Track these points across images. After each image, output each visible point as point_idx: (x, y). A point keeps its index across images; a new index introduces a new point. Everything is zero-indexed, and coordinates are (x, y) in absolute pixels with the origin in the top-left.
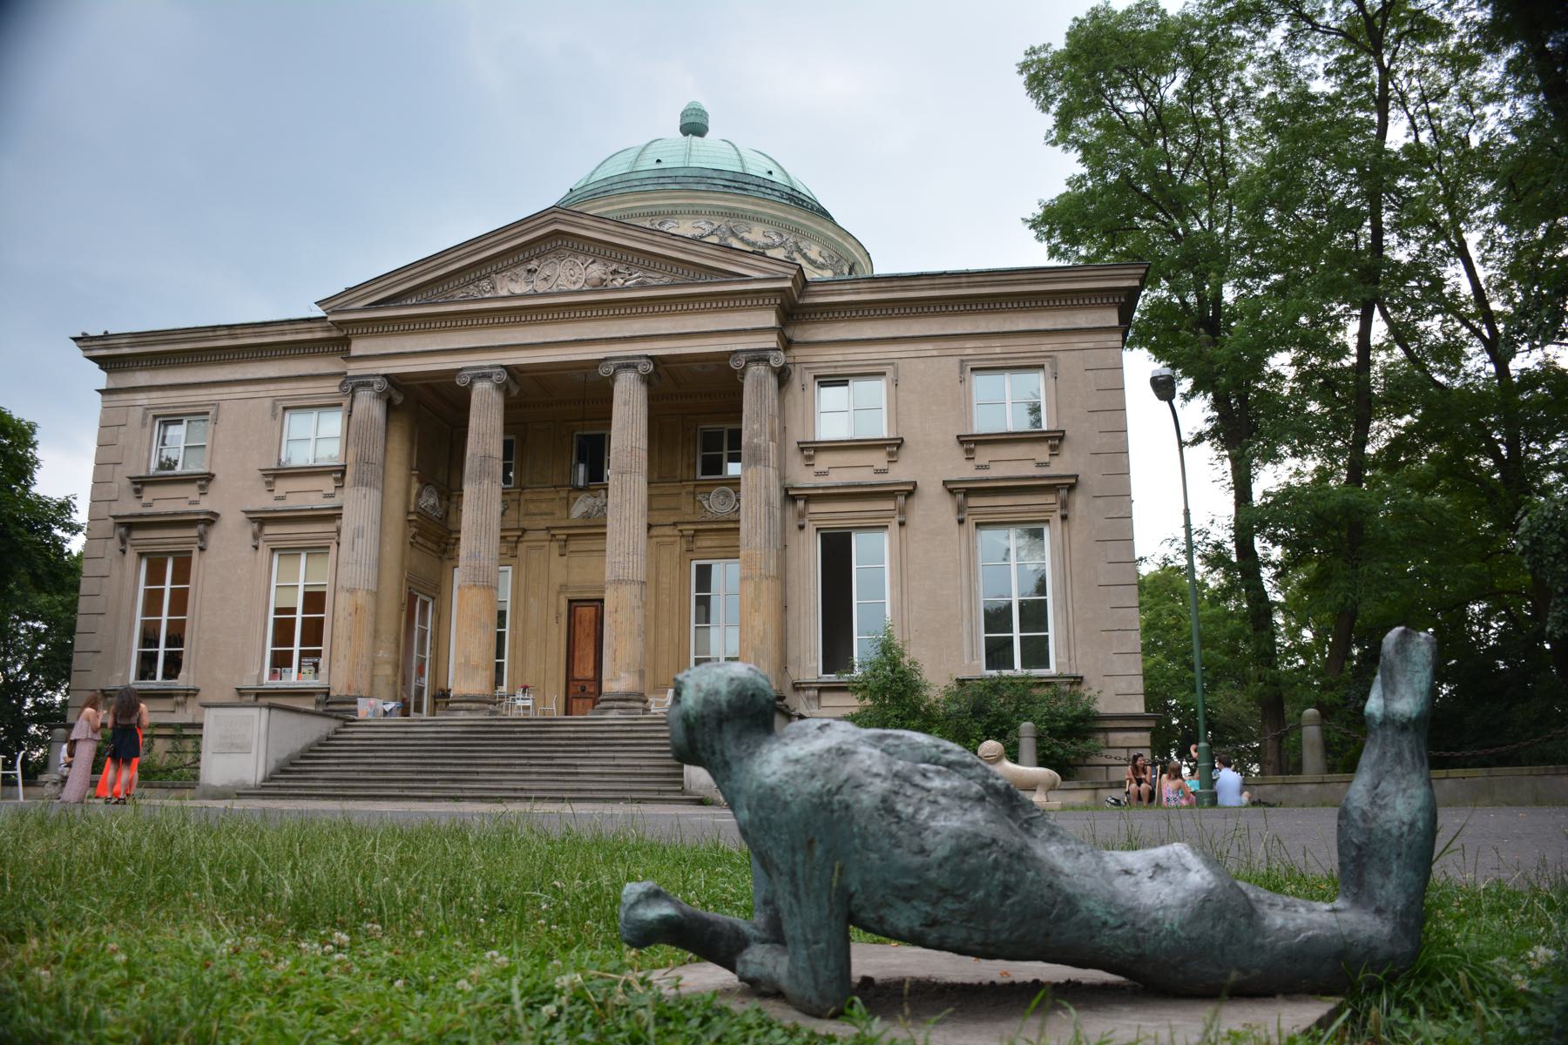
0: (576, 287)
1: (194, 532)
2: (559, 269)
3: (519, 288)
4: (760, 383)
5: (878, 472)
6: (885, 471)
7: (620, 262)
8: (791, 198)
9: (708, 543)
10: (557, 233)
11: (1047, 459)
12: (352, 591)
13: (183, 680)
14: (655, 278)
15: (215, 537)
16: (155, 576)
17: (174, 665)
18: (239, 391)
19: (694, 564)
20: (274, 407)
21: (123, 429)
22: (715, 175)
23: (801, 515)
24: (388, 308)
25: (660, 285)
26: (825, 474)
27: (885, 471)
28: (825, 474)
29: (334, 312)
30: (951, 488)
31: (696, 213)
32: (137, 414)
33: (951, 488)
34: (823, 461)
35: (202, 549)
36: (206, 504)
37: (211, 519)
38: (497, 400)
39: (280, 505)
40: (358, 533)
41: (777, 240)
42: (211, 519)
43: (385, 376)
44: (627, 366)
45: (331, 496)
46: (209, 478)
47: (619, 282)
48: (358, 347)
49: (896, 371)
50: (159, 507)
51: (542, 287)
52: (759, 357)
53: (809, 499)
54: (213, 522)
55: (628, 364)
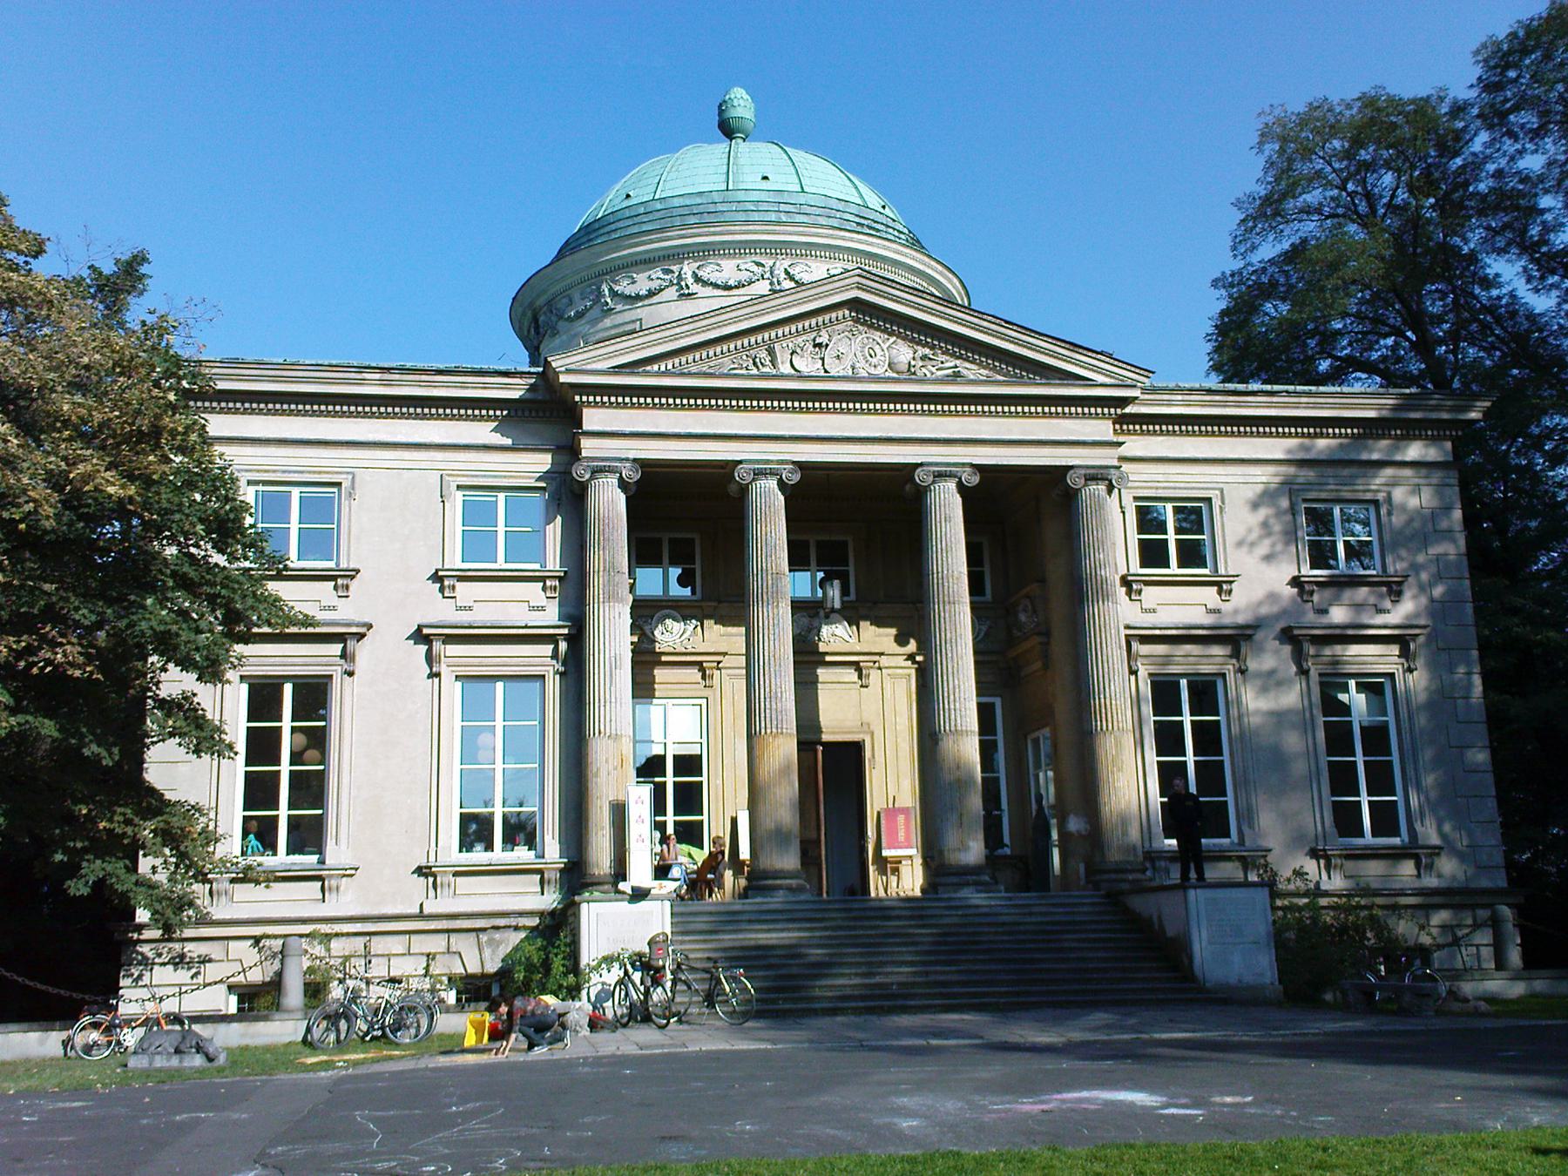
0: (879, 371)
1: (336, 649)
3: (806, 364)
5: (1210, 611)
7: (926, 345)
12: (616, 737)
14: (970, 370)
17: (308, 836)
22: (841, 206)
25: (976, 377)
29: (568, 371)
34: (1151, 595)
35: (351, 674)
39: (464, 617)
40: (616, 665)
43: (635, 460)
44: (951, 475)
45: (543, 609)
46: (353, 574)
47: (929, 371)
48: (593, 418)
52: (1097, 475)
54: (362, 636)
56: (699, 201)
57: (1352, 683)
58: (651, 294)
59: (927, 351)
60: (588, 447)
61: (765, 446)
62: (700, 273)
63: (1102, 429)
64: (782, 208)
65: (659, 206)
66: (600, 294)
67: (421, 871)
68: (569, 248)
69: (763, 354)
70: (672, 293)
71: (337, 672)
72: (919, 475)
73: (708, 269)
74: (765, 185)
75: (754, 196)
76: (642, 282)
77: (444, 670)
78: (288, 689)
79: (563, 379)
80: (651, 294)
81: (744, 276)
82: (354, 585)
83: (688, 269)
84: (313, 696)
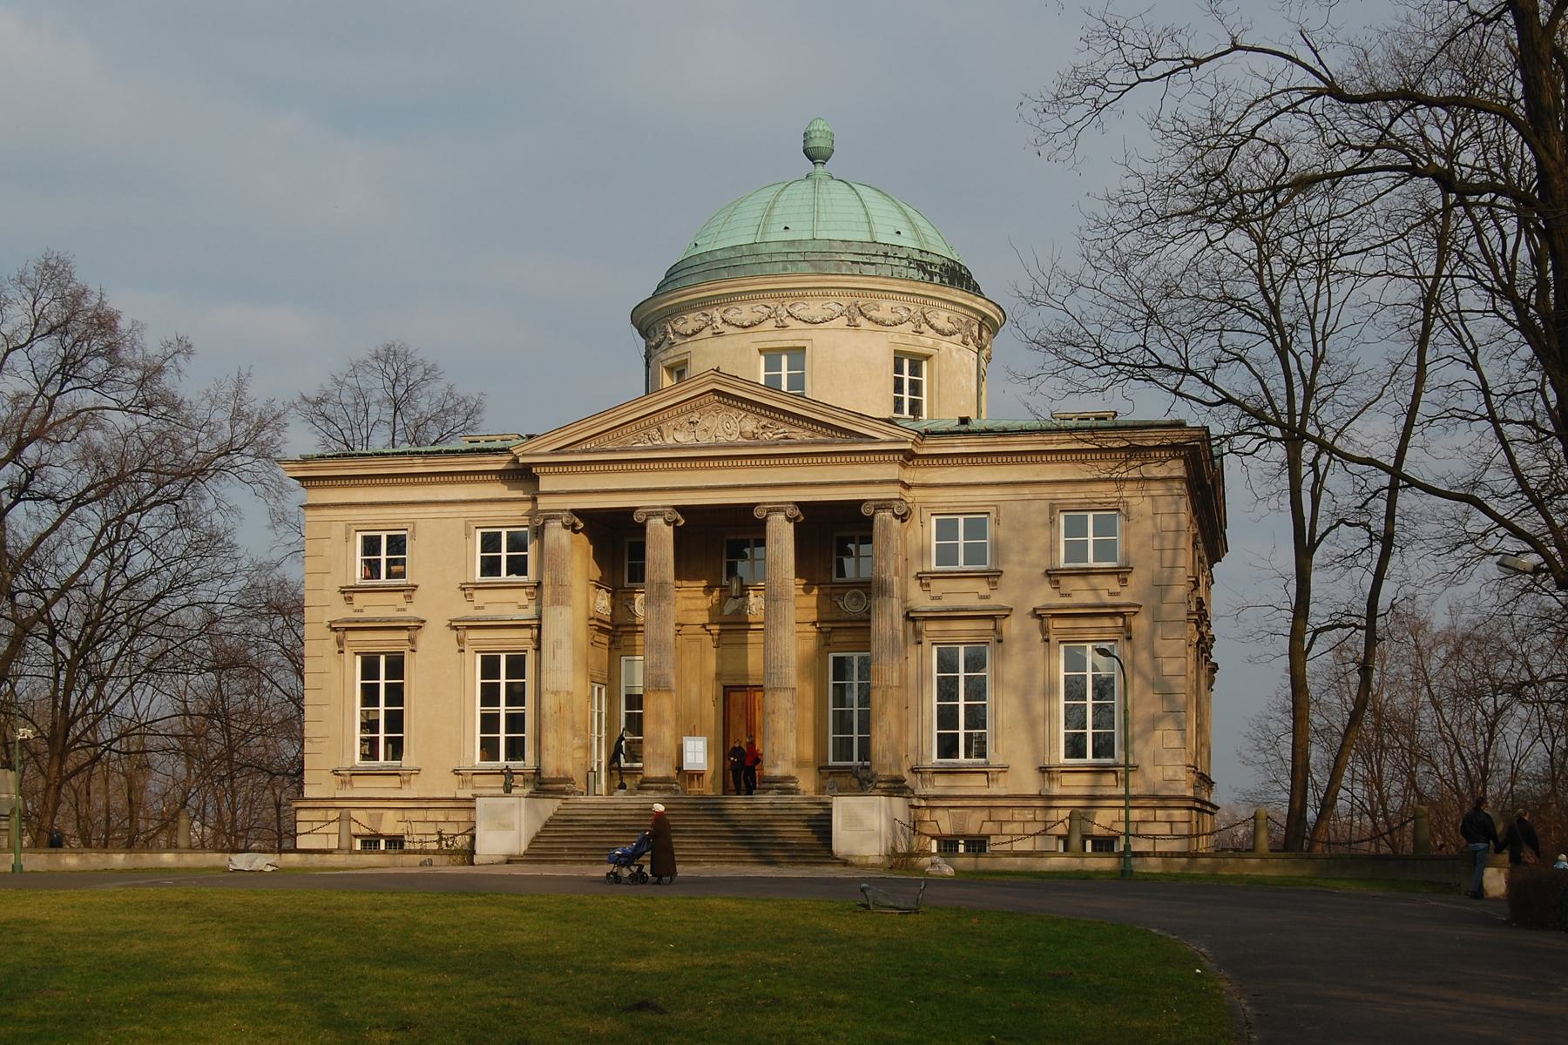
0: (733, 438)
1: (405, 635)
2: (718, 421)
3: (682, 438)
4: (886, 525)
5: (981, 597)
6: (987, 597)
8: (921, 266)
9: (843, 639)
10: (715, 391)
11: (1118, 589)
12: (556, 693)
13: (408, 761)
14: (800, 434)
15: (423, 639)
16: (370, 669)
18: (433, 511)
19: (831, 656)
20: (467, 527)
21: (327, 542)
23: (918, 633)
24: (572, 453)
26: (939, 598)
27: (987, 597)
28: (939, 598)
30: (1037, 614)
31: (825, 292)
32: (338, 531)
33: (1037, 614)
34: (938, 586)
36: (412, 611)
37: (420, 625)
38: (669, 530)
39: (479, 613)
40: (558, 644)
41: (905, 314)
42: (420, 625)
44: (778, 510)
48: (546, 484)
49: (998, 513)
50: (369, 613)
51: (704, 440)
52: (884, 505)
53: (927, 619)
55: (776, 508)
56: (733, 254)
57: (1089, 647)
58: (695, 333)
59: (764, 422)
60: (544, 503)
61: (655, 495)
62: (726, 317)
63: (892, 471)
64: (791, 257)
65: (708, 258)
66: (666, 333)
67: (456, 772)
68: (673, 275)
69: (654, 432)
70: (707, 332)
71: (406, 650)
72: (758, 513)
73: (732, 312)
74: (788, 236)
75: (773, 248)
76: (691, 321)
77: (467, 648)
78: (382, 659)
79: (522, 460)
80: (695, 333)
81: (755, 317)
82: (416, 595)
83: (716, 314)
84: (396, 666)
